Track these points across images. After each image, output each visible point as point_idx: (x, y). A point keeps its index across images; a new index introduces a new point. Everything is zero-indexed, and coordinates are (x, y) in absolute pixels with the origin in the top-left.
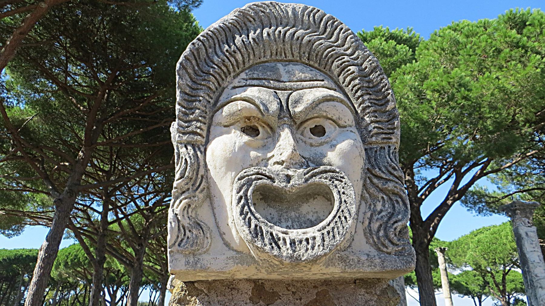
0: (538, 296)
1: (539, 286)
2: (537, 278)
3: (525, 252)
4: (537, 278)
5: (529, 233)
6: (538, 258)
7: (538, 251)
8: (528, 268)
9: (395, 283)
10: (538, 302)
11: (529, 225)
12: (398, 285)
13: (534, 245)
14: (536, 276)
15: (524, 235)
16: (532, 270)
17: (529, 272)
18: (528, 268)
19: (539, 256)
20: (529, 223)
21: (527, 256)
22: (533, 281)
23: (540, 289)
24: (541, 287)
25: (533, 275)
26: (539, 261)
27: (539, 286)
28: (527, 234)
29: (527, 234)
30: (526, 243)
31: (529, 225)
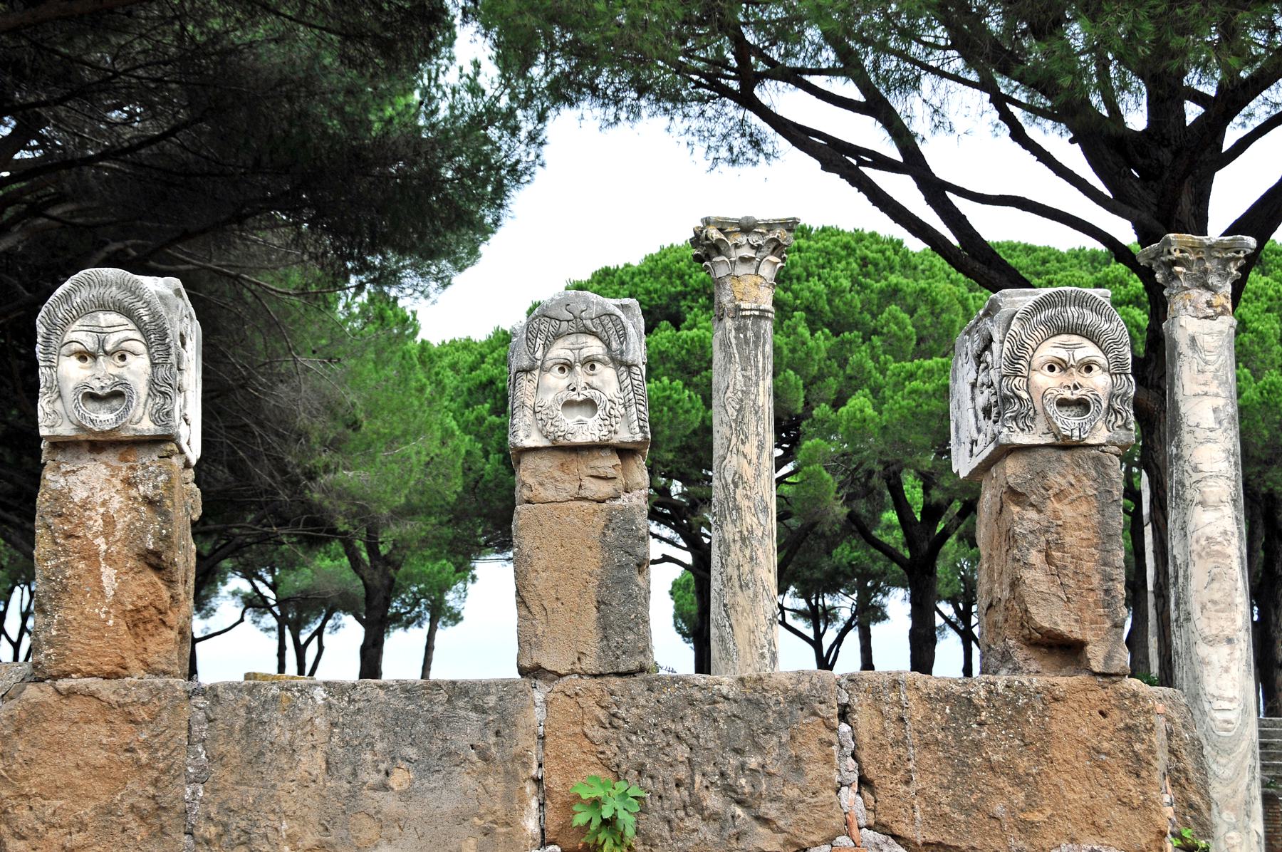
0: (1190, 528)
1: (1198, 498)
2: (1196, 477)
3: (1179, 397)
4: (1196, 477)
6: (1211, 415)
7: (1217, 395)
8: (1178, 447)
9: (740, 491)
10: (1186, 546)
11: (1210, 312)
12: (748, 498)
13: (1209, 375)
14: (1196, 469)
16: (1186, 453)
17: (1179, 457)
18: (1178, 447)
20: (1209, 304)
21: (1183, 410)
22: (1183, 486)
24: (1202, 503)
25: (1187, 467)
28: (1193, 339)
30: (1185, 369)
31: (1210, 312)
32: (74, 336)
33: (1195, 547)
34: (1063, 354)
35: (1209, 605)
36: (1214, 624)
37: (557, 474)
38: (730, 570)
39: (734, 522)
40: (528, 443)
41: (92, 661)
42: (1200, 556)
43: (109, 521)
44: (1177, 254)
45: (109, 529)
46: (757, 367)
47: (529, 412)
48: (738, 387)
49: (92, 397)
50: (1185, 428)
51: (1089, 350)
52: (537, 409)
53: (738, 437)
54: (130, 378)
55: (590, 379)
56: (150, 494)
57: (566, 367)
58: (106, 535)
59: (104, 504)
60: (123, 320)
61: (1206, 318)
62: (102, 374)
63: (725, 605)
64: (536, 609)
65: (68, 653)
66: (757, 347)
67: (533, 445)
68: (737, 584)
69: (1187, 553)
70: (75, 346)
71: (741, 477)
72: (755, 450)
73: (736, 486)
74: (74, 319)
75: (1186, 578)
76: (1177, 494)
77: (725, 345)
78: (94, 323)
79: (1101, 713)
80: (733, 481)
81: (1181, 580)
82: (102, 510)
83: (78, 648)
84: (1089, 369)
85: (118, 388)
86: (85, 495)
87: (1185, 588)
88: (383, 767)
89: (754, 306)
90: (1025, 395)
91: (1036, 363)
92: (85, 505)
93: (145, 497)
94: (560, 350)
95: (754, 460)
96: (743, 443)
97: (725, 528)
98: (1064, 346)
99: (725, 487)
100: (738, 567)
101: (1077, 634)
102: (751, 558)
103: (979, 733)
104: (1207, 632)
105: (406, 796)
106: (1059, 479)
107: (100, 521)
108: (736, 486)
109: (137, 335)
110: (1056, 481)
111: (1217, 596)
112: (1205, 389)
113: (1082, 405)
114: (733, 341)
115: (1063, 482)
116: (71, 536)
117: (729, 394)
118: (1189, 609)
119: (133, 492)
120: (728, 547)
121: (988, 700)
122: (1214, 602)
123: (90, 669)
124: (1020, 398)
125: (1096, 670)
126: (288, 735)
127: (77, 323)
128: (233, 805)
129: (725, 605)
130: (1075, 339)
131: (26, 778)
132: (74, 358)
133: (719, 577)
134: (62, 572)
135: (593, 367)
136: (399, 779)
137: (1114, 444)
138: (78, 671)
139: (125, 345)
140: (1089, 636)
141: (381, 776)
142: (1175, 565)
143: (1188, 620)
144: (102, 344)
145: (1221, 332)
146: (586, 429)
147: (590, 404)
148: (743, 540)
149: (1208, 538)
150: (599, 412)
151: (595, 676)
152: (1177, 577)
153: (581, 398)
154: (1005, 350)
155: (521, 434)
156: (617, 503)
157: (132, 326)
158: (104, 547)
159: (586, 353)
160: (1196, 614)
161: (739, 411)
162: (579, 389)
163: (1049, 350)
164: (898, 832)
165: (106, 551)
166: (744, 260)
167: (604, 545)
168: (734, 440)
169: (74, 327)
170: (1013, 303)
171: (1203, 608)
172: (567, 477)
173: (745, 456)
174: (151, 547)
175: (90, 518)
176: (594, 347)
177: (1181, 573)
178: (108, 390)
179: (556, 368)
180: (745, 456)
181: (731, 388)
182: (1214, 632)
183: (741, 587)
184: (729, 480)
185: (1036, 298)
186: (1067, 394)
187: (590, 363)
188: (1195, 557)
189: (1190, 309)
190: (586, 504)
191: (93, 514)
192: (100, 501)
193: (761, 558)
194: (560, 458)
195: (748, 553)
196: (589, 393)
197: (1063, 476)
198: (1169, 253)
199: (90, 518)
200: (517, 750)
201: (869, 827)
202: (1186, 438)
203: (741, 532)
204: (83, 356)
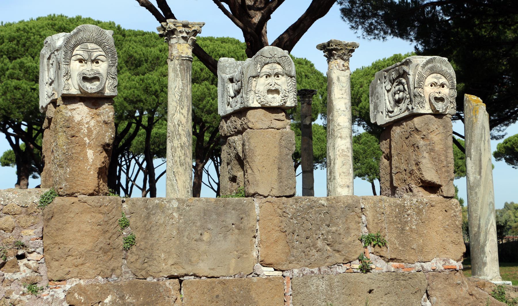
0: (336, 146)
1: (339, 135)
2: (339, 128)
3: (333, 98)
4: (339, 128)
5: (341, 78)
7: (345, 98)
9: (180, 128)
10: (334, 152)
11: (344, 68)
13: (343, 91)
14: (339, 125)
15: (335, 80)
16: (335, 119)
17: (333, 120)
18: (332, 116)
19: (345, 104)
20: (343, 65)
21: (334, 103)
22: (334, 131)
23: (340, 139)
24: (341, 137)
26: (345, 109)
27: (339, 135)
28: (338, 78)
29: (338, 78)
30: (336, 88)
31: (344, 68)
32: (78, 52)
33: (338, 153)
34: (436, 81)
35: (342, 174)
36: (343, 181)
37: (263, 118)
38: (176, 158)
39: (178, 139)
40: (252, 105)
41: (84, 188)
42: (339, 156)
43: (90, 130)
44: (334, 46)
45: (90, 134)
46: (187, 80)
47: (253, 93)
48: (180, 87)
49: (85, 79)
50: (335, 110)
51: (443, 80)
52: (257, 92)
53: (180, 107)
54: (101, 71)
55: (276, 81)
56: (106, 120)
57: (268, 76)
58: (89, 136)
59: (87, 123)
60: (98, 47)
61: (343, 70)
62: (88, 68)
63: (174, 172)
64: (255, 171)
65: (74, 185)
66: (187, 72)
67: (254, 106)
68: (179, 164)
69: (335, 155)
70: (79, 57)
71: (181, 122)
72: (186, 112)
73: (179, 126)
74: (78, 45)
75: (334, 164)
76: (332, 133)
77: (175, 70)
78: (86, 47)
79: (446, 211)
80: (178, 124)
81: (332, 165)
82: (87, 126)
83: (78, 183)
84: (443, 87)
85: (96, 75)
86: (80, 119)
87: (334, 167)
88: (200, 232)
89: (187, 56)
90: (423, 95)
91: (426, 84)
92: (79, 123)
93: (104, 121)
94: (266, 69)
95: (186, 116)
96: (182, 109)
97: (174, 142)
98: (436, 78)
99: (174, 126)
100: (180, 157)
101: (439, 183)
102: (185, 154)
103: (407, 218)
104: (341, 183)
105: (210, 243)
106: (432, 126)
107: (86, 131)
108: (179, 126)
109: (103, 53)
110: (433, 127)
111: (345, 171)
112: (342, 96)
113: (441, 99)
114: (178, 69)
115: (434, 127)
116: (73, 136)
117: (176, 90)
118: (335, 175)
119: (99, 119)
120: (176, 149)
121: (411, 206)
122: (344, 173)
123: (83, 192)
124: (421, 96)
125: (445, 195)
126: (163, 220)
127: (79, 47)
128: (142, 247)
129: (174, 172)
130: (439, 75)
131: (57, 236)
132: (77, 62)
133: (171, 161)
134: (71, 151)
135: (278, 77)
136: (206, 237)
137: (450, 114)
138: (79, 192)
139: (99, 57)
140: (443, 184)
141: (199, 236)
142: (330, 159)
143: (334, 179)
144: (90, 56)
145: (347, 76)
146: (276, 101)
147: (277, 91)
148: (182, 146)
149: (342, 150)
150: (281, 94)
151: (277, 197)
152: (330, 164)
153: (274, 88)
154: (416, 78)
155: (250, 102)
156: (284, 130)
157: (101, 50)
158: (88, 141)
159: (276, 71)
160: (337, 177)
161: (180, 96)
162: (273, 85)
163: (431, 79)
164: (382, 255)
165: (89, 143)
166: (183, 37)
167: (280, 146)
168: (178, 108)
169: (77, 49)
170: (417, 61)
171: (340, 175)
172: (266, 119)
173: (183, 114)
174: (108, 142)
175: (82, 129)
176: (279, 69)
177: (332, 162)
178: (93, 76)
179: (265, 76)
180: (183, 114)
181: (177, 88)
182: (343, 183)
183: (181, 165)
184: (176, 123)
185: (427, 59)
186: (437, 96)
187: (277, 75)
188: (338, 156)
189: (337, 67)
190: (273, 130)
191: (83, 127)
192: (85, 122)
193: (188, 154)
194: (263, 111)
195: (183, 152)
196: (277, 87)
197: (434, 125)
198: (332, 46)
199: (82, 129)
200: (250, 225)
201: (373, 253)
202: (335, 113)
203: (181, 144)
204: (81, 61)
